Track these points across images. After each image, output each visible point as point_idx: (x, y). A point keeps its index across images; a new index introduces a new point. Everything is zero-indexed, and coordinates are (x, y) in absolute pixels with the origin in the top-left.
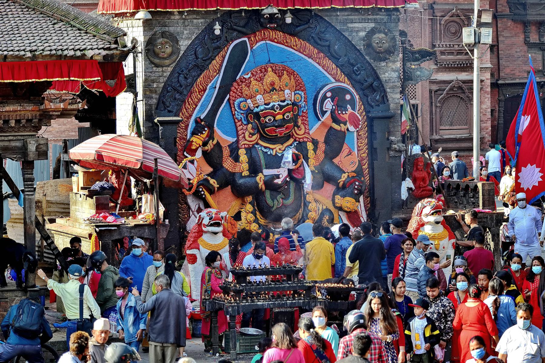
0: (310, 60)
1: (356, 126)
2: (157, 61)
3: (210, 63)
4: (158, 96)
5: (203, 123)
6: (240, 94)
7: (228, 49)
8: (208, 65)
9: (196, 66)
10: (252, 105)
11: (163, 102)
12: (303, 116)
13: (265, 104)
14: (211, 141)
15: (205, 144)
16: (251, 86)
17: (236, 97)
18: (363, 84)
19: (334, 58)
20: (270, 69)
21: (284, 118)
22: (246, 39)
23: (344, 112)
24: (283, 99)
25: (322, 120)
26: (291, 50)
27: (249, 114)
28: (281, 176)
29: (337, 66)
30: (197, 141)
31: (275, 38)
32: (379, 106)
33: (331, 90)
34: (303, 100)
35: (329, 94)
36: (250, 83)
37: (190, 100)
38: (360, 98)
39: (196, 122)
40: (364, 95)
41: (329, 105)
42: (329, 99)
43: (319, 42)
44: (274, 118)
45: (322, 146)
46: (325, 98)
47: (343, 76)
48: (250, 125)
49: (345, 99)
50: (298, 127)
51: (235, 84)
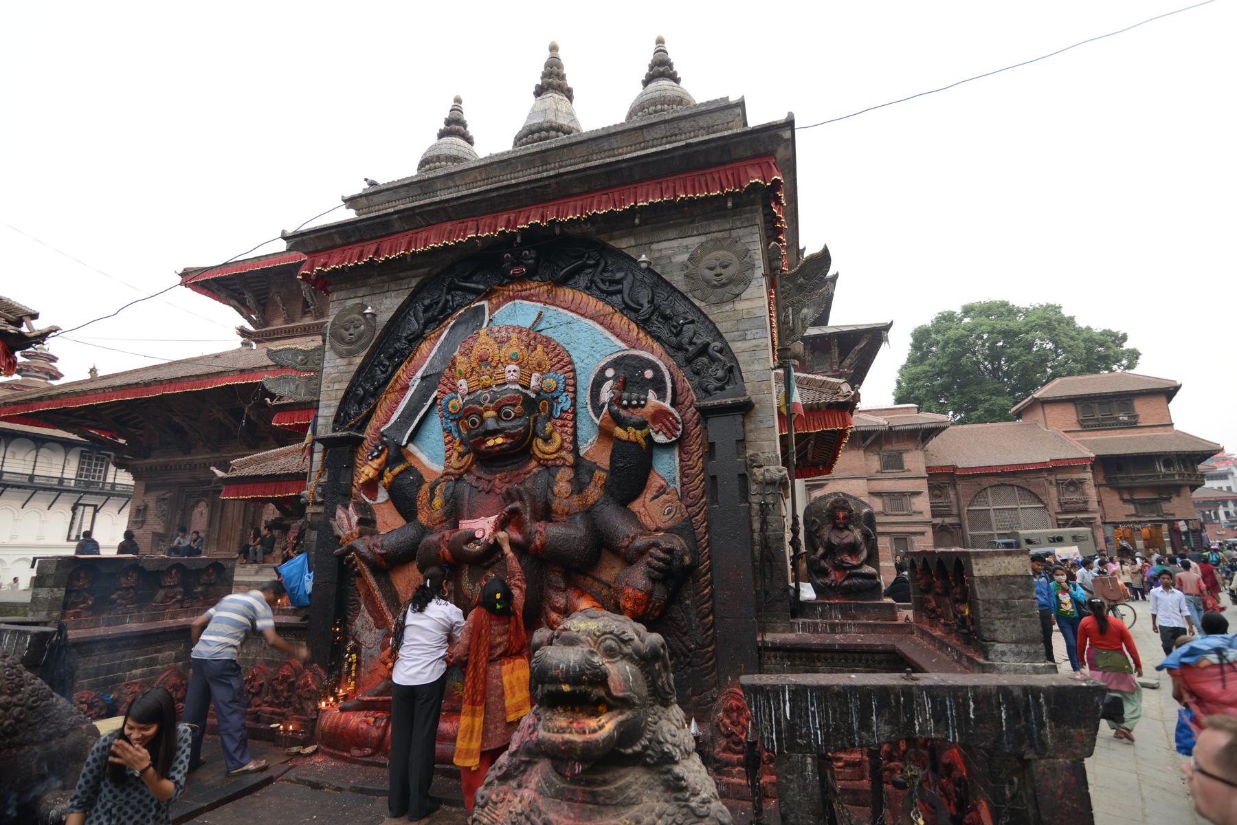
1: (669, 432)
2: (343, 348)
11: (347, 414)
12: (560, 418)
18: (687, 350)
22: (485, 303)
23: (635, 402)
25: (598, 422)
28: (478, 535)
30: (367, 471)
32: (722, 388)
34: (561, 386)
35: (610, 373)
43: (604, 288)
44: (480, 415)
49: (644, 379)
50: (547, 439)
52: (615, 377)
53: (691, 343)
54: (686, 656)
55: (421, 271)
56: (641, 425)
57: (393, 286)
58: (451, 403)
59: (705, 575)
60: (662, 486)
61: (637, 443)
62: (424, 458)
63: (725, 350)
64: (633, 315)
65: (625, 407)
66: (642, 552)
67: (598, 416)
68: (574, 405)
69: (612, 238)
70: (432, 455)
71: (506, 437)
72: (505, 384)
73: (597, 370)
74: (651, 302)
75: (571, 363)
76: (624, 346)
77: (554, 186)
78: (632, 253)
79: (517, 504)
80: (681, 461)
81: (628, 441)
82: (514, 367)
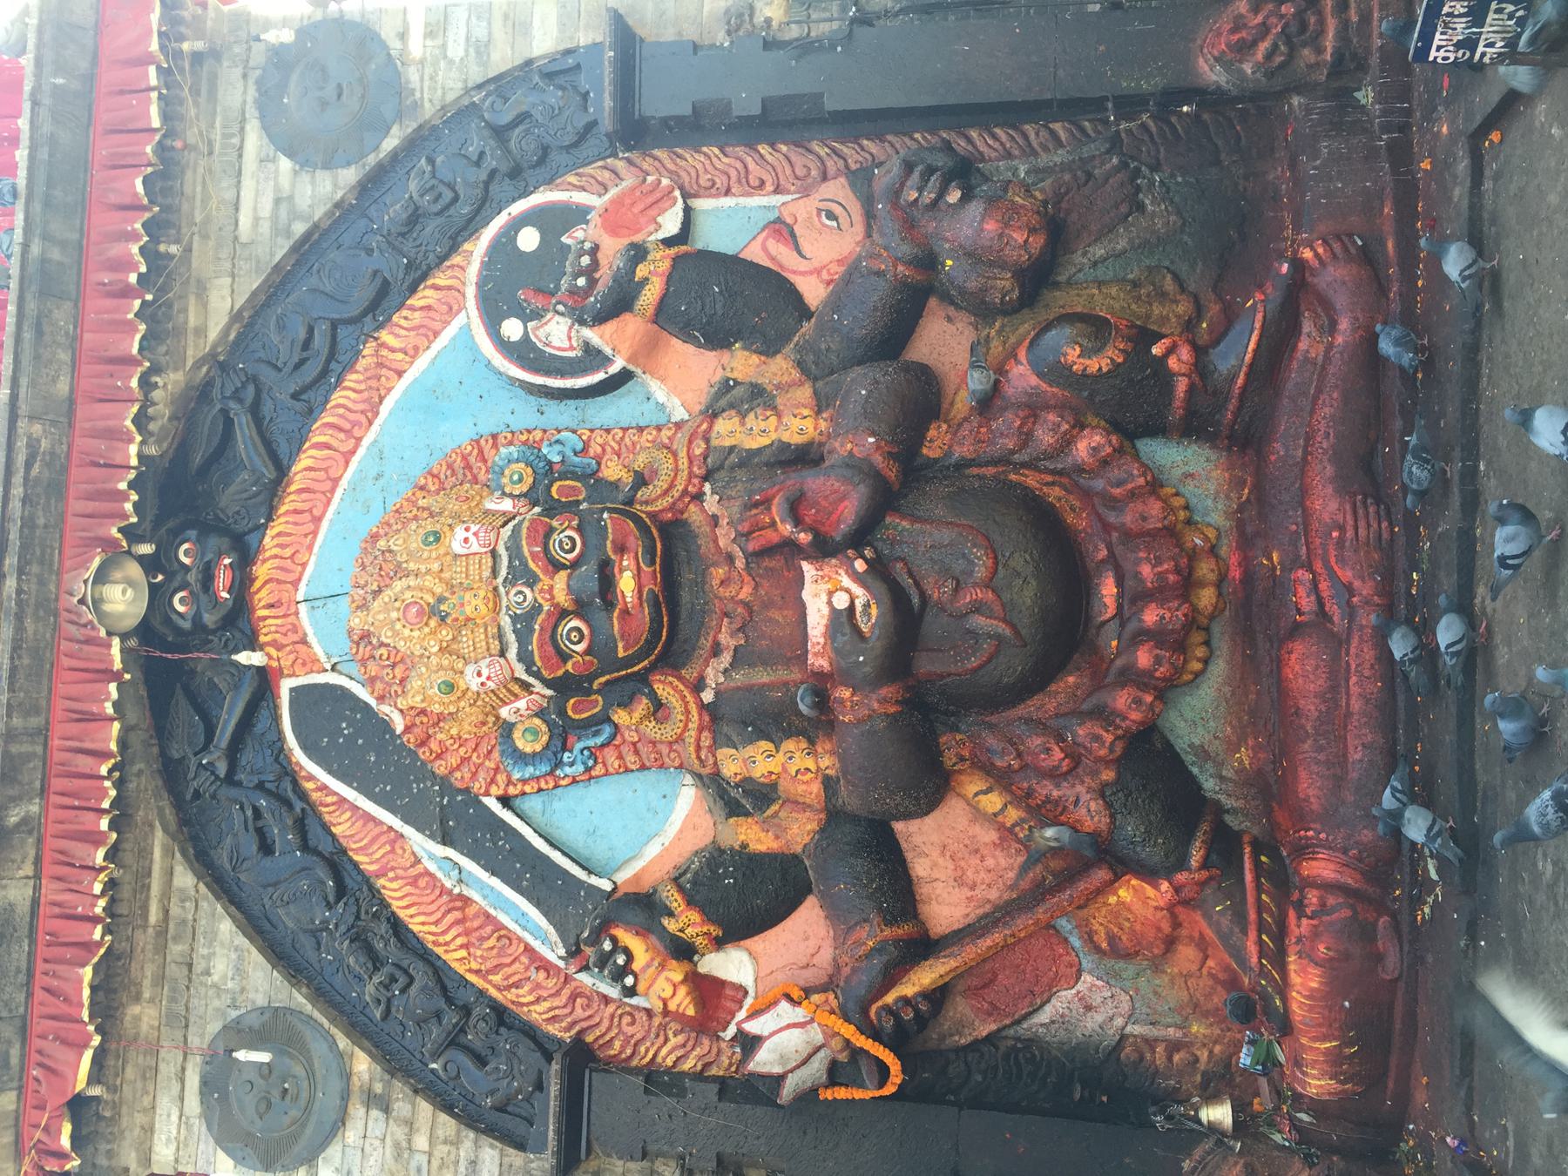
0: (385, 409)
1: (660, 201)
3: (356, 865)
4: (472, 1135)
5: (589, 951)
6: (484, 749)
7: (311, 778)
8: (364, 876)
9: (360, 939)
10: (521, 704)
11: (501, 1109)
13: (502, 654)
14: (665, 921)
15: (683, 951)
16: (437, 708)
17: (497, 770)
18: (492, 174)
19: (382, 301)
20: (356, 622)
21: (575, 565)
22: (286, 686)
23: (585, 260)
24: (487, 561)
26: (339, 492)
27: (562, 713)
28: (841, 601)
29: (413, 290)
30: (664, 987)
31: (292, 557)
32: (585, 96)
33: (493, 322)
35: (512, 329)
36: (423, 712)
37: (496, 978)
38: (550, 182)
39: (585, 968)
40: (542, 161)
41: (557, 334)
42: (530, 325)
45: (742, 363)
46: (524, 353)
47: (456, 259)
48: (620, 716)
51: (440, 768)
52: (525, 319)
53: (478, 164)
54: (1137, 173)
55: (157, 853)
56: (638, 253)
57: (176, 949)
58: (524, 744)
59: (969, 140)
60: (778, 232)
61: (676, 260)
62: (653, 850)
63: (500, 85)
64: (393, 298)
65: (592, 282)
66: (909, 225)
67: (608, 361)
68: (574, 432)
69: (201, 332)
70: (641, 821)
71: (621, 549)
72: (494, 553)
73: (500, 361)
74: (369, 252)
75: (477, 442)
76: (460, 320)
77: (37, 429)
78: (251, 283)
79: (778, 508)
80: (728, 192)
81: (669, 280)
82: (460, 533)
